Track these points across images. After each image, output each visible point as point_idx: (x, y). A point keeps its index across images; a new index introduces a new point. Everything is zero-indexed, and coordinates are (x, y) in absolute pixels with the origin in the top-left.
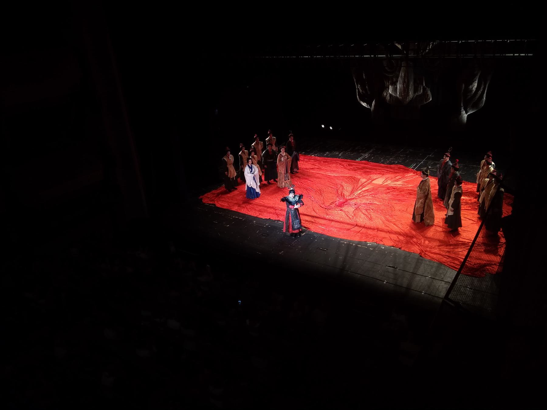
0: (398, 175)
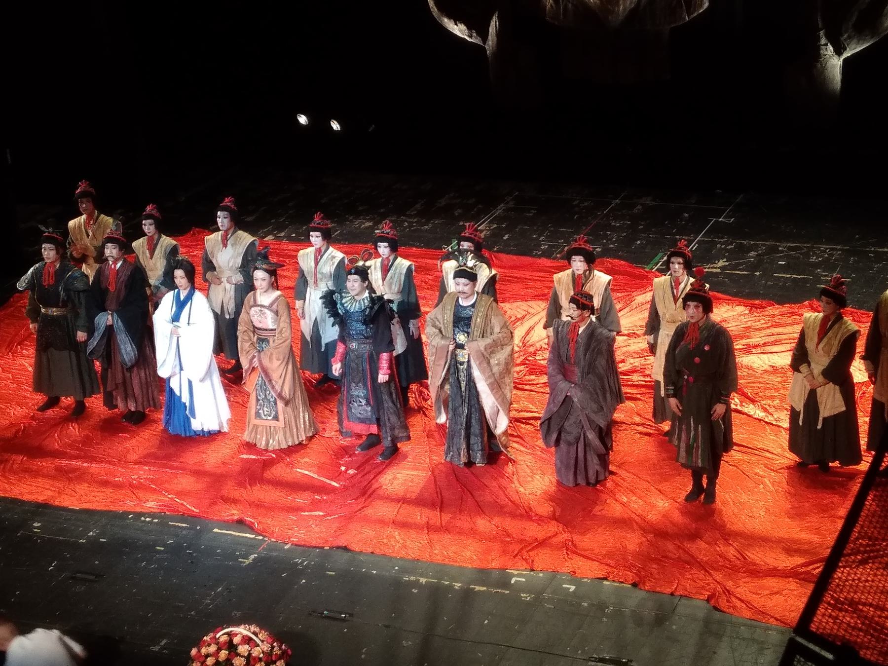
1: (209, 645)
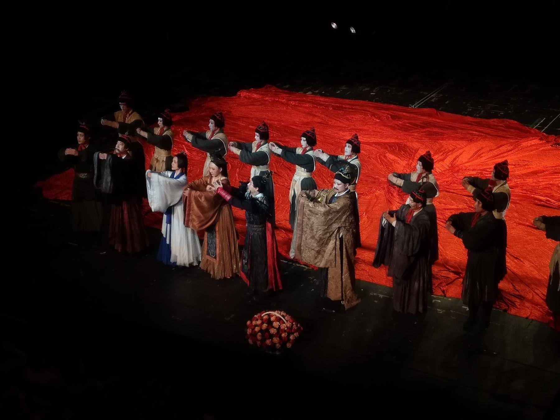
0: (504, 142)
1: (257, 320)
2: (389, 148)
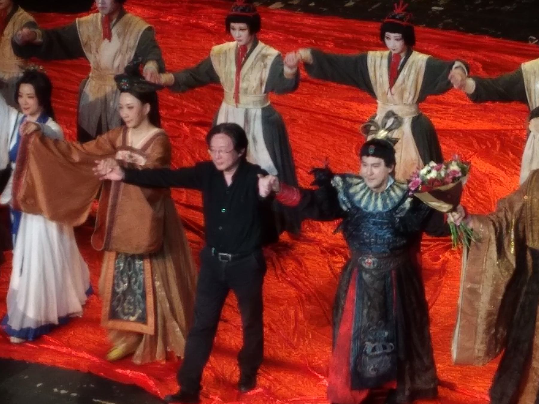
2: (476, 146)
